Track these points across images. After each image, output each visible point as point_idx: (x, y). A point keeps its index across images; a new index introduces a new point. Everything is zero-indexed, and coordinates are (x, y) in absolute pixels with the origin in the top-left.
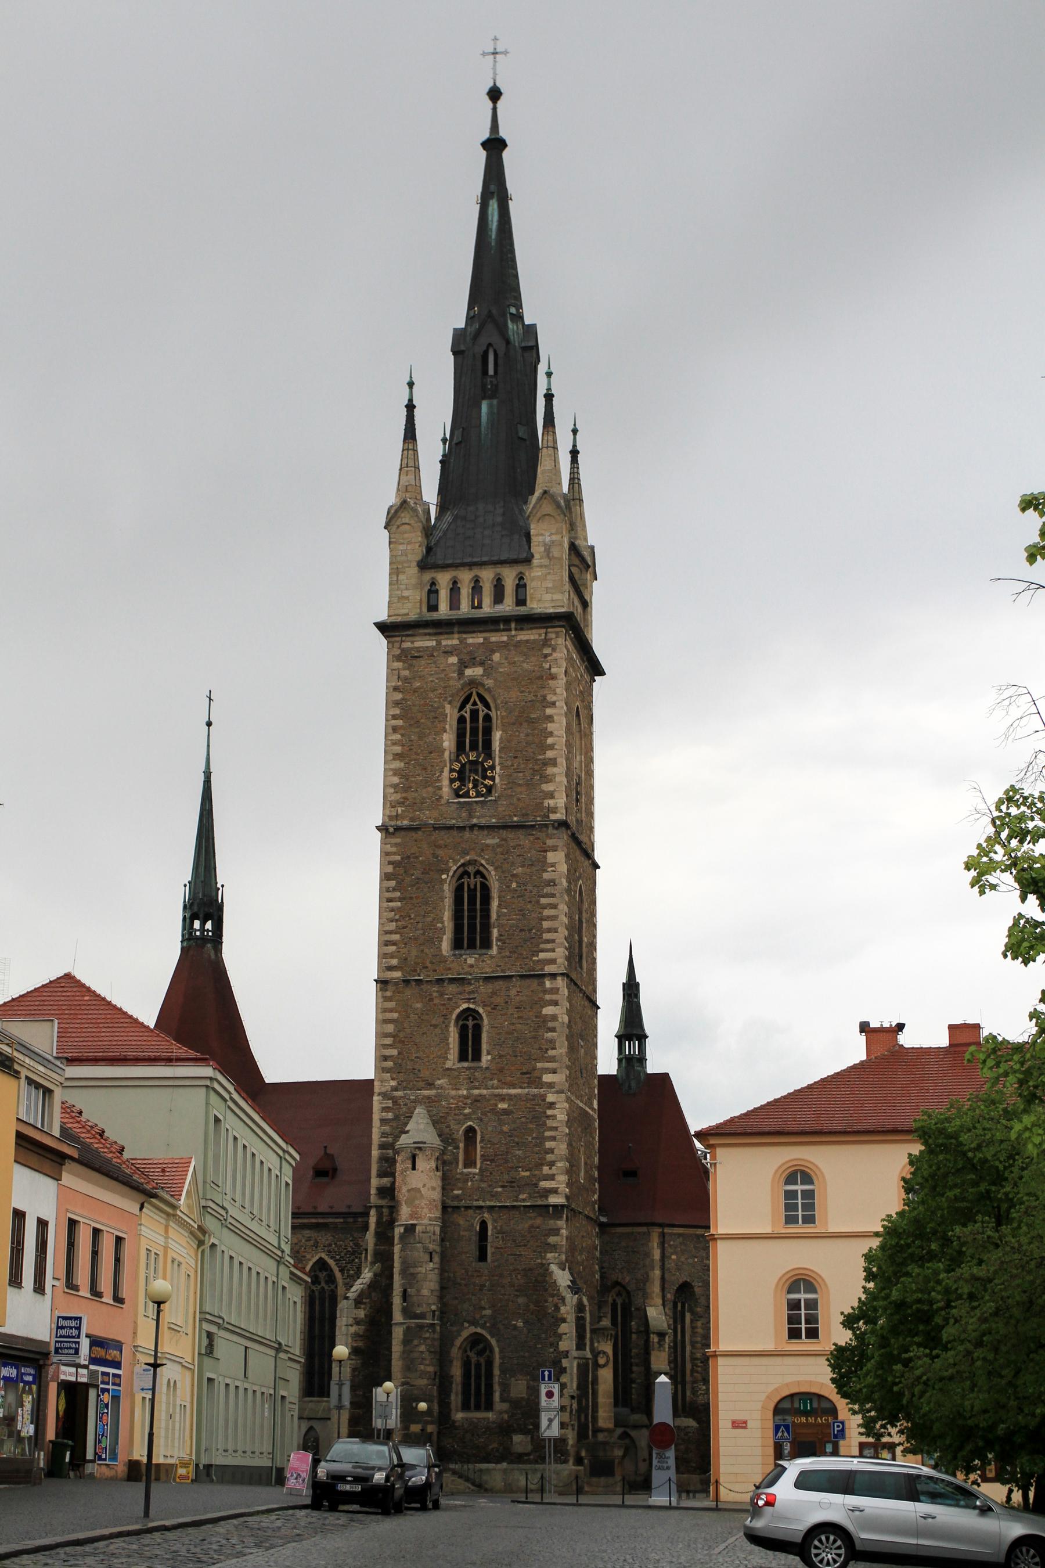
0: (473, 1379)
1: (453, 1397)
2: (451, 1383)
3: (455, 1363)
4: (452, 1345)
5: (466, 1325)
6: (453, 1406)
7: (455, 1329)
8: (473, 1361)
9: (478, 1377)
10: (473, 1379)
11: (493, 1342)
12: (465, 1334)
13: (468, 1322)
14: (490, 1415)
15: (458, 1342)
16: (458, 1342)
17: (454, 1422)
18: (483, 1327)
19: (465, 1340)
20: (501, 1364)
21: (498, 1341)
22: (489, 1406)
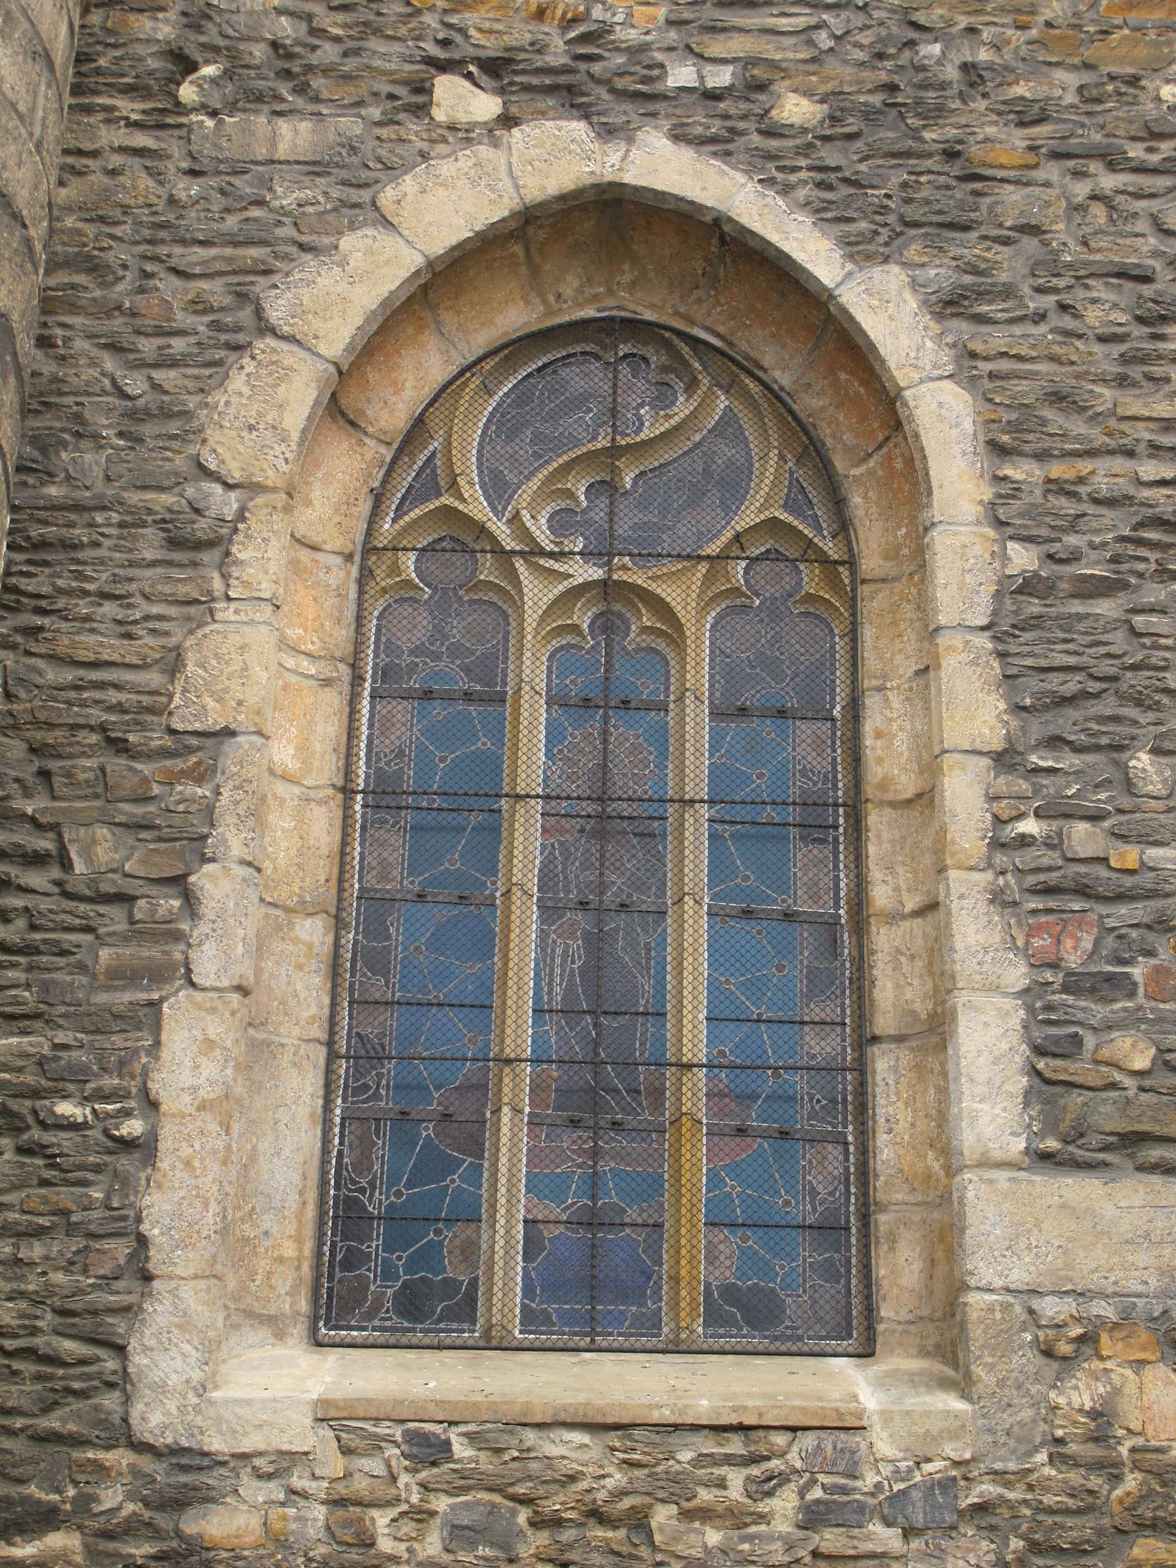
0: (526, 844)
1: (189, 1057)
2: (187, 845)
3: (261, 558)
4: (238, 328)
5: (462, 100)
6: (175, 1204)
7: (293, 136)
8: (536, 595)
9: (610, 820)
10: (526, 844)
11: (888, 310)
12: (447, 202)
13: (495, 69)
14: (883, 1403)
15: (338, 292)
16: (338, 292)
17: (188, 1475)
18: (727, 122)
19: (443, 283)
20: (1020, 617)
21: (949, 306)
22: (817, 1270)
